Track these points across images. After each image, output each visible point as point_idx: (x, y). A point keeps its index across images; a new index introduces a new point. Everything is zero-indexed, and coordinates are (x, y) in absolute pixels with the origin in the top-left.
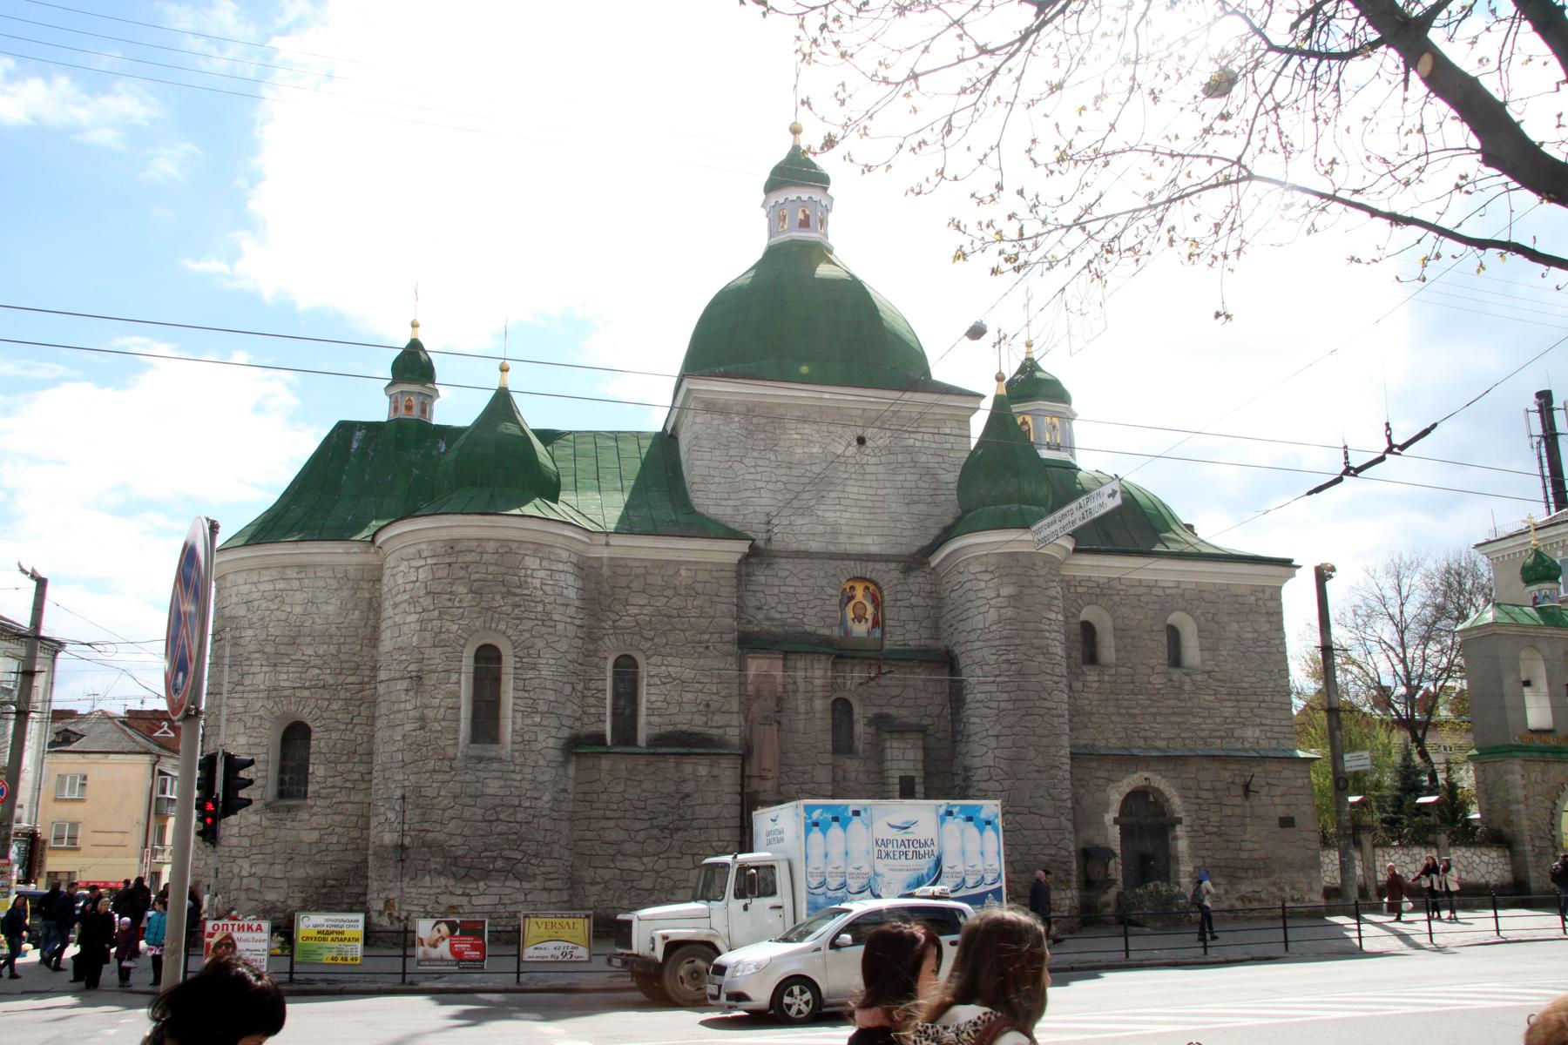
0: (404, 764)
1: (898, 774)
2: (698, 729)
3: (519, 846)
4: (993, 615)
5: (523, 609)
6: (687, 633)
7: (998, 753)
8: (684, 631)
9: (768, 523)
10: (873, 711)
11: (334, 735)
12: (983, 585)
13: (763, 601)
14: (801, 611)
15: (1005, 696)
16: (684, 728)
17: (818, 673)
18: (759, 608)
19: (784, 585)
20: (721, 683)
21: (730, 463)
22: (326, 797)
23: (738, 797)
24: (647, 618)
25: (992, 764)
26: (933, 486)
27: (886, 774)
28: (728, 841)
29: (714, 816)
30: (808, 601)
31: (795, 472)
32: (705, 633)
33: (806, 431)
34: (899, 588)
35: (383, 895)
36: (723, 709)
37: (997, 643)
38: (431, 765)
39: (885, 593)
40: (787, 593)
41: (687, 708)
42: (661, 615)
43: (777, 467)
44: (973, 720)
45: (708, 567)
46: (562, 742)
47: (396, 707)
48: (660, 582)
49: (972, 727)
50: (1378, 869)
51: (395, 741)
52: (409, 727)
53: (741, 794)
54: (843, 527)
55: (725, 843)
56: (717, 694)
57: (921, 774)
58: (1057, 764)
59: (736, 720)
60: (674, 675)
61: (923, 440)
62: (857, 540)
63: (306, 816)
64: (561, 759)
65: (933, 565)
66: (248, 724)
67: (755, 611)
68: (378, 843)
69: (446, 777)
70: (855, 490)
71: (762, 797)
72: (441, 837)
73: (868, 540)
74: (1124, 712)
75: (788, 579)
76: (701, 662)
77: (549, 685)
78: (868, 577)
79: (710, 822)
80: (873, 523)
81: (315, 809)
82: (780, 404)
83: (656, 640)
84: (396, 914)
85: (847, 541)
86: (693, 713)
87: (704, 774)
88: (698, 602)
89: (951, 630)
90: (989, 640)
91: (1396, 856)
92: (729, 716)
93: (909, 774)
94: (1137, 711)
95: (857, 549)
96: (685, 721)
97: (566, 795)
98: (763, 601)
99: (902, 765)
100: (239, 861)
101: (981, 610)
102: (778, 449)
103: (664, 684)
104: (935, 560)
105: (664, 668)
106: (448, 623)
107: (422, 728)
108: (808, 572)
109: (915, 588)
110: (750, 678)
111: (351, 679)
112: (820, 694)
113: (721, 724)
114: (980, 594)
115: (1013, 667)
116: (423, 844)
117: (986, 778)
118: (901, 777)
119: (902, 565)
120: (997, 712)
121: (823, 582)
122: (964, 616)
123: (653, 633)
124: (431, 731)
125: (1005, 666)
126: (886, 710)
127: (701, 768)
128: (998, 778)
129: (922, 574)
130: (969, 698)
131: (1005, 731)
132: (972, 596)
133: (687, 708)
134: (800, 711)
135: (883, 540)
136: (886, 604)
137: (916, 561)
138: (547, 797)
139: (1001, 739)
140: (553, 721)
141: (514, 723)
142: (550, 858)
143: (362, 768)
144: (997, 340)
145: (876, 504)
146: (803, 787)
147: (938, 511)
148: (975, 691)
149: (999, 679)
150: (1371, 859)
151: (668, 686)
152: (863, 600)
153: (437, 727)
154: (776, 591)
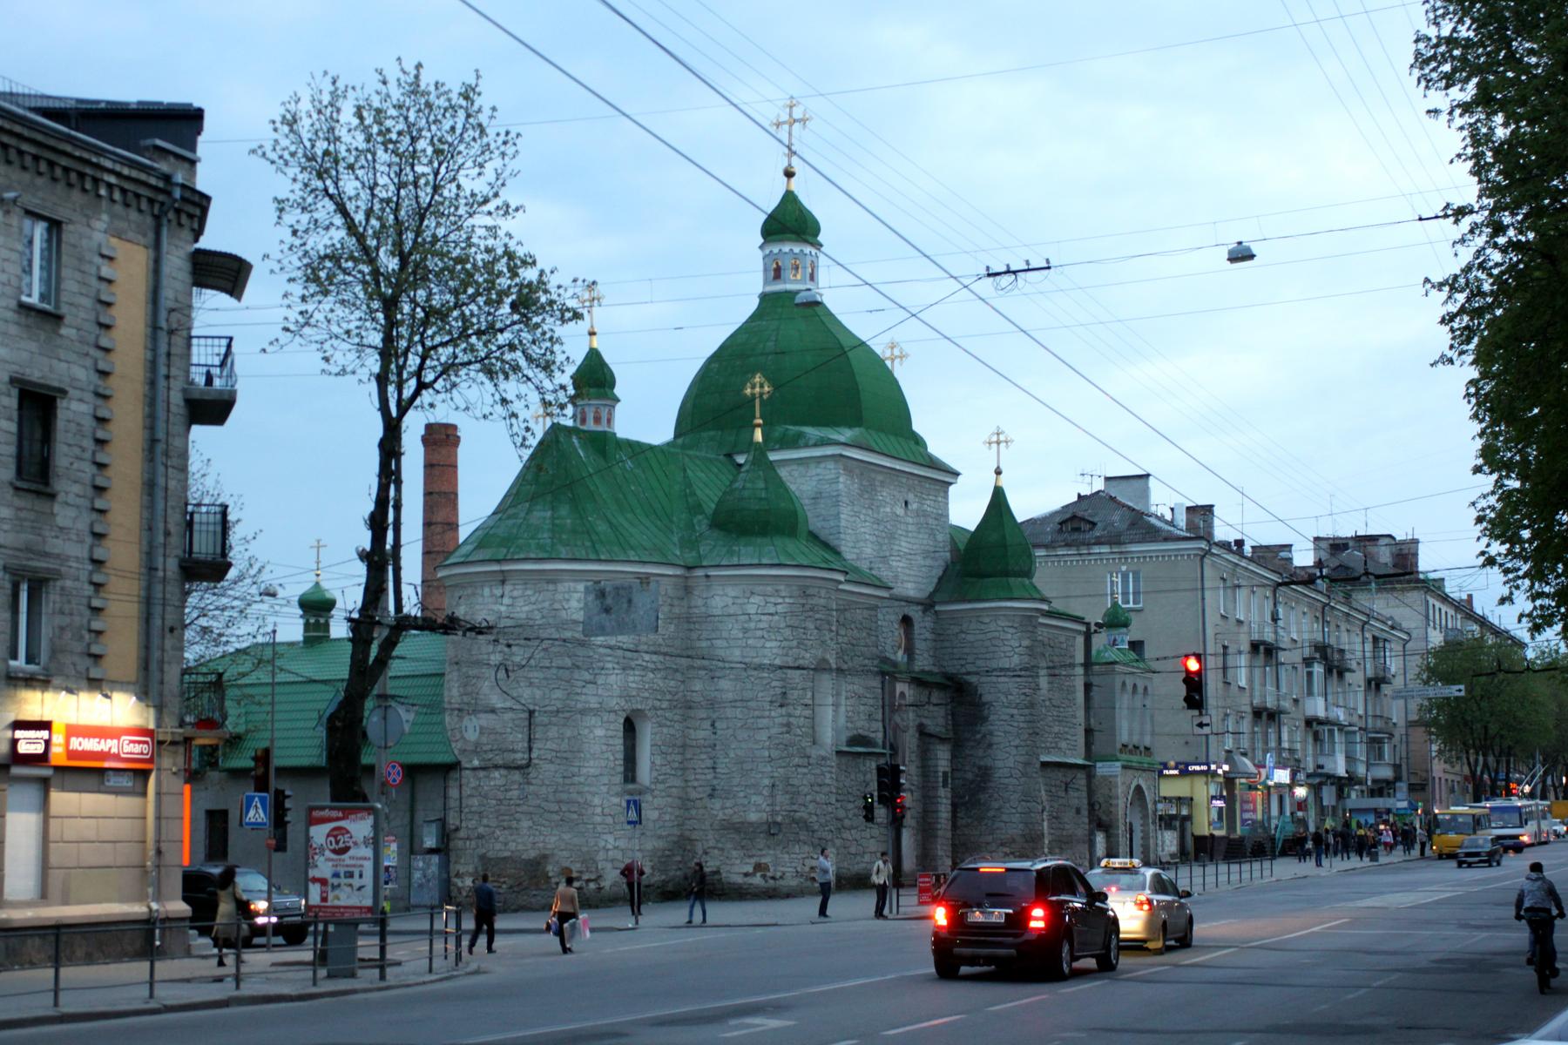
0: (771, 759)
2: (866, 733)
7: (1018, 758)
9: (871, 569)
11: (665, 730)
12: (1009, 636)
16: (861, 731)
22: (663, 782)
31: (881, 528)
35: (753, 861)
38: (796, 761)
47: (757, 713)
51: (757, 742)
52: (774, 731)
59: (881, 729)
62: (906, 585)
63: (650, 799)
66: (605, 719)
68: (736, 819)
69: (805, 770)
70: (903, 544)
72: (805, 815)
73: (909, 585)
81: (656, 793)
84: (769, 874)
89: (963, 662)
93: (947, 769)
100: (605, 837)
106: (803, 652)
107: (788, 732)
111: (672, 683)
116: (794, 821)
122: (988, 656)
124: (795, 735)
125: (1023, 697)
126: (925, 721)
130: (992, 717)
132: (995, 642)
137: (928, 605)
143: (679, 758)
144: (995, 438)
147: (936, 564)
153: (799, 732)
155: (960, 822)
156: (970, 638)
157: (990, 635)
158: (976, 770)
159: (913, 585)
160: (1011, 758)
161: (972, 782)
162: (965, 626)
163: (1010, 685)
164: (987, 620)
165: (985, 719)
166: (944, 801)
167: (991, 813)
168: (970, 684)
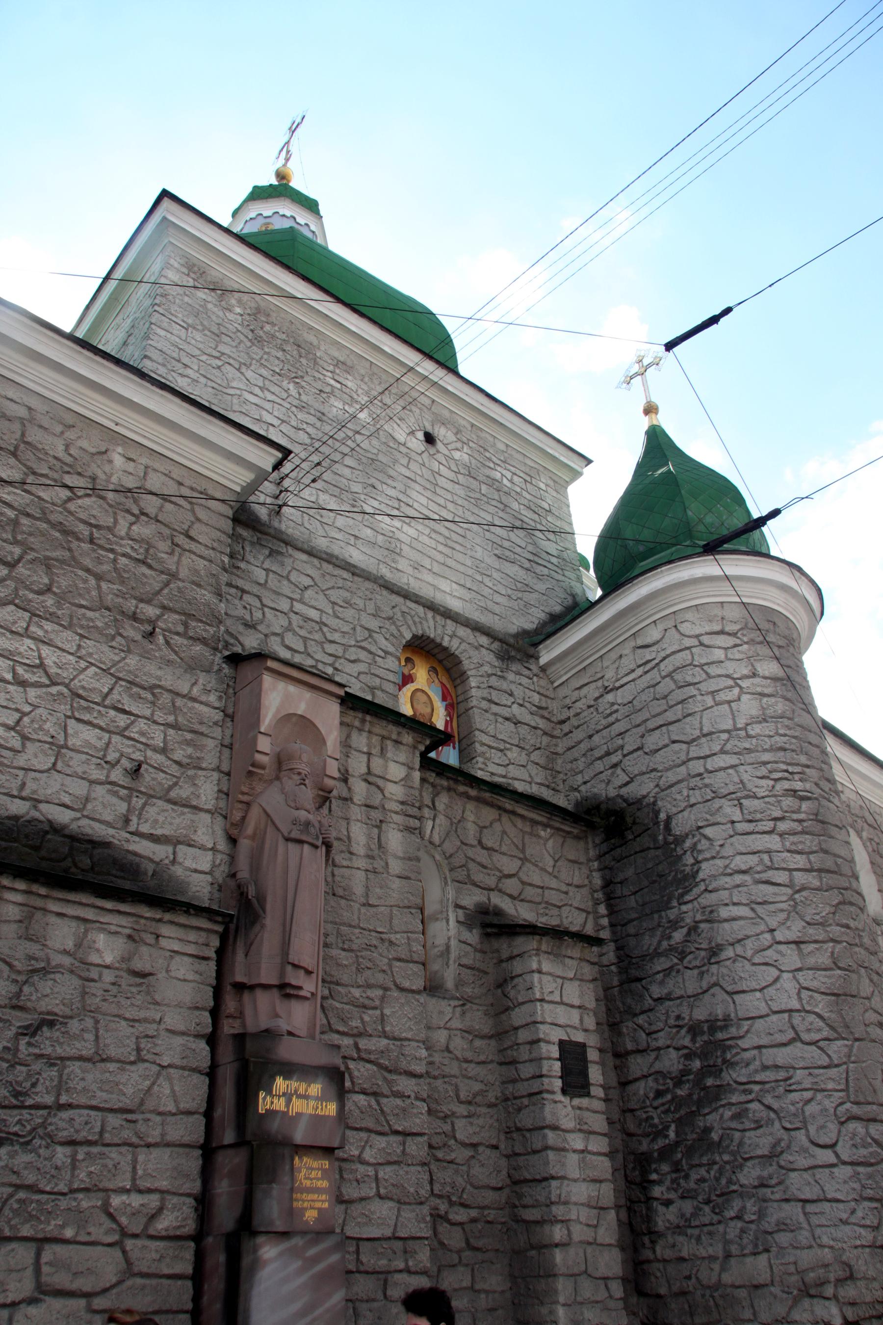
1: (557, 1035)
2: (99, 831)
4: (749, 707)
6: (104, 585)
7: (806, 978)
8: (99, 577)
10: (472, 898)
13: (258, 615)
14: (330, 660)
15: (800, 861)
16: (63, 816)
17: (396, 771)
18: (251, 626)
19: (301, 601)
20: (176, 726)
21: (220, 363)
23: (202, 1047)
24: (11, 514)
25: (798, 1006)
26: (530, 548)
27: (523, 1036)
28: (162, 1192)
29: (126, 1102)
30: (346, 647)
32: (149, 602)
33: (349, 384)
34: (494, 681)
36: (173, 794)
37: (766, 757)
39: (473, 682)
40: (307, 619)
41: (77, 762)
42: (48, 522)
43: (301, 408)
44: (724, 913)
45: (176, 473)
48: (61, 454)
49: (726, 925)
53: (212, 1040)
54: (404, 547)
55: (153, 1201)
56: (164, 751)
57: (592, 1041)
60: (53, 670)
61: (511, 481)
62: (429, 578)
65: (543, 661)
67: (241, 628)
71: (286, 1050)
73: (445, 585)
75: (309, 593)
76: (132, 661)
78: (445, 643)
79: (114, 1121)
80: (450, 562)
82: (311, 328)
83: (21, 570)
85: (410, 570)
86: (92, 782)
87: (108, 959)
88: (144, 530)
89: (614, 759)
90: (749, 751)
92: (189, 815)
93: (579, 1037)
95: (426, 592)
96: (67, 800)
98: (258, 615)
99: (562, 1015)
101: (723, 696)
102: (303, 384)
103: (23, 684)
104: (547, 655)
105: (28, 642)
108: (347, 595)
109: (518, 692)
110: (267, 721)
112: (397, 818)
113: (166, 831)
114: (713, 670)
115: (805, 806)
117: (784, 1038)
118: (561, 1043)
119: (496, 645)
120: (789, 891)
121: (374, 624)
122: (670, 716)
123: (17, 551)
125: (788, 802)
126: (497, 900)
127: (101, 940)
128: (816, 1036)
129: (527, 672)
130: (706, 869)
131: (813, 932)
133: (77, 762)
134: (355, 848)
135: (468, 596)
136: (474, 702)
139: (808, 948)
145: (454, 537)
146: (363, 1043)
147: (541, 587)
148: (728, 851)
149: (782, 826)
151: (32, 693)
152: (426, 689)
154: (284, 605)
155: (665, 1217)
156: (621, 696)
157: (667, 667)
158: (687, 1042)
159: (459, 592)
160: (787, 982)
161: (679, 1082)
162: (610, 674)
163: (747, 774)
164: (654, 634)
165: (688, 880)
166: (577, 1142)
167: (749, 1175)
168: (638, 803)
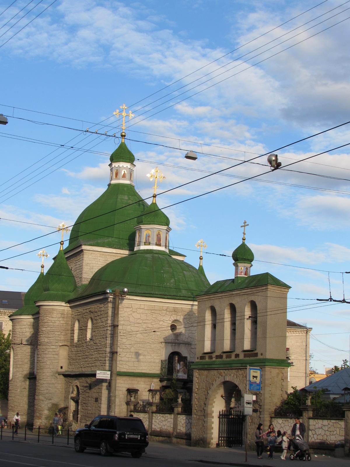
3: (13, 403)
5: (16, 340)
46: (23, 375)
50: (153, 423)
58: (41, 378)
64: (23, 380)
74: (79, 358)
77: (20, 360)
91: (159, 418)
94: (80, 358)
97: (25, 389)
138: (19, 390)
140: (21, 369)
141: (13, 371)
142: (20, 406)
150: (151, 418)
